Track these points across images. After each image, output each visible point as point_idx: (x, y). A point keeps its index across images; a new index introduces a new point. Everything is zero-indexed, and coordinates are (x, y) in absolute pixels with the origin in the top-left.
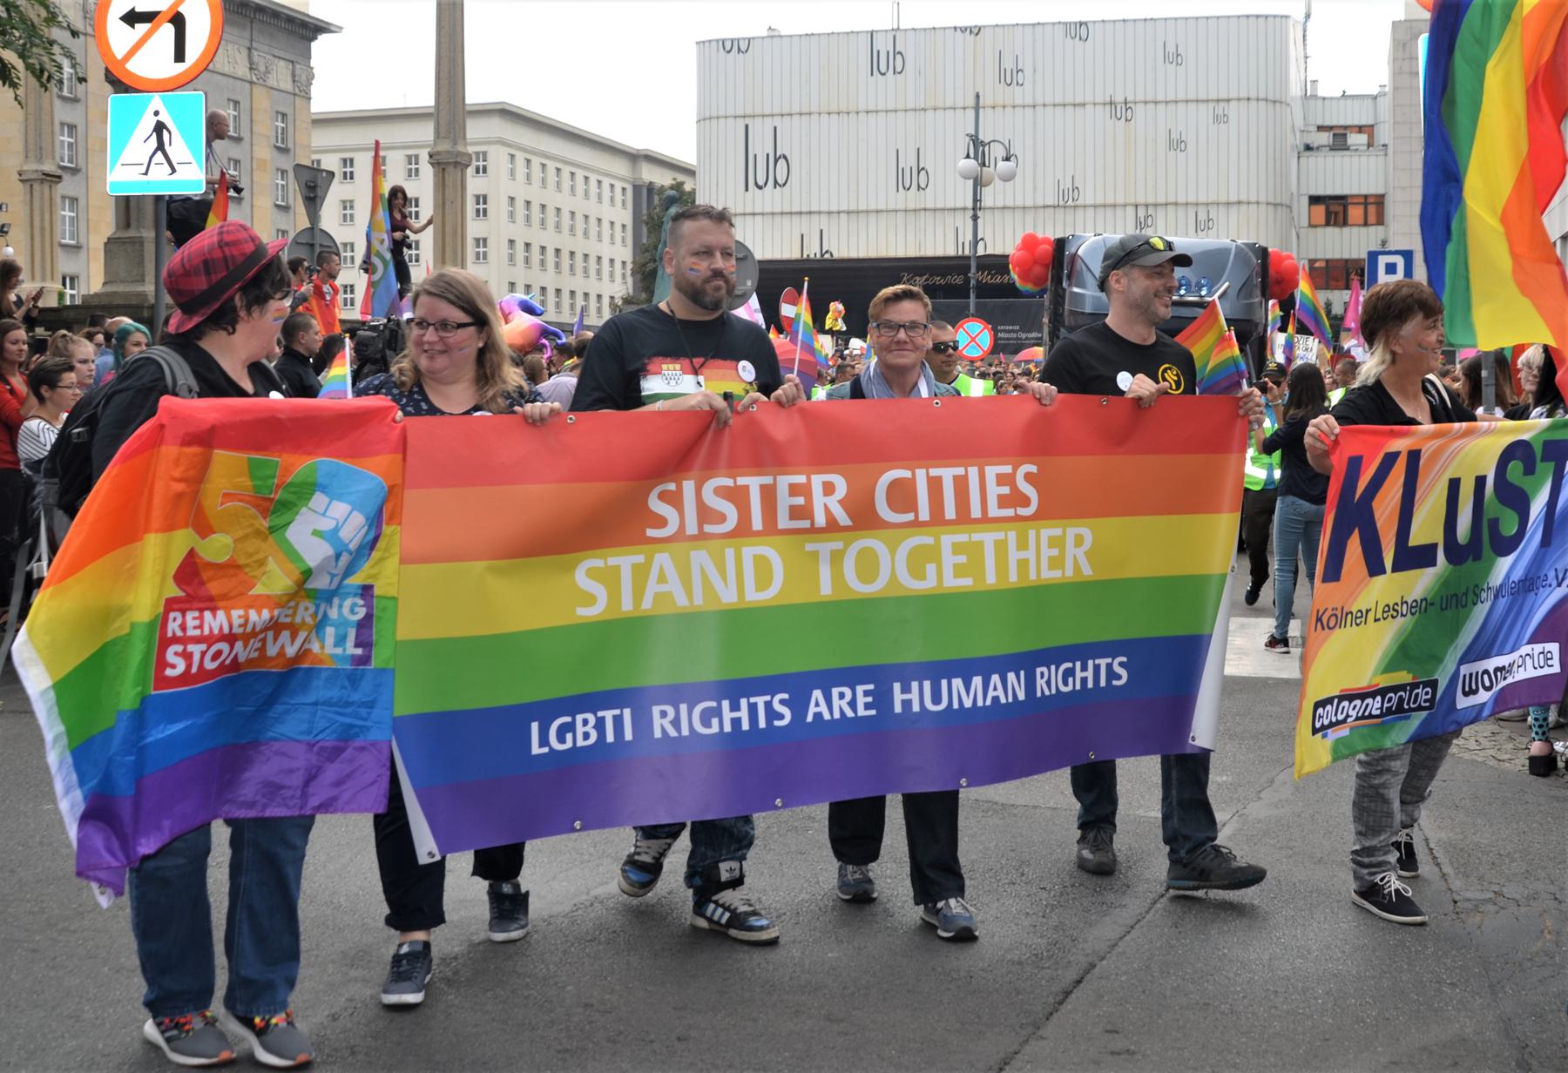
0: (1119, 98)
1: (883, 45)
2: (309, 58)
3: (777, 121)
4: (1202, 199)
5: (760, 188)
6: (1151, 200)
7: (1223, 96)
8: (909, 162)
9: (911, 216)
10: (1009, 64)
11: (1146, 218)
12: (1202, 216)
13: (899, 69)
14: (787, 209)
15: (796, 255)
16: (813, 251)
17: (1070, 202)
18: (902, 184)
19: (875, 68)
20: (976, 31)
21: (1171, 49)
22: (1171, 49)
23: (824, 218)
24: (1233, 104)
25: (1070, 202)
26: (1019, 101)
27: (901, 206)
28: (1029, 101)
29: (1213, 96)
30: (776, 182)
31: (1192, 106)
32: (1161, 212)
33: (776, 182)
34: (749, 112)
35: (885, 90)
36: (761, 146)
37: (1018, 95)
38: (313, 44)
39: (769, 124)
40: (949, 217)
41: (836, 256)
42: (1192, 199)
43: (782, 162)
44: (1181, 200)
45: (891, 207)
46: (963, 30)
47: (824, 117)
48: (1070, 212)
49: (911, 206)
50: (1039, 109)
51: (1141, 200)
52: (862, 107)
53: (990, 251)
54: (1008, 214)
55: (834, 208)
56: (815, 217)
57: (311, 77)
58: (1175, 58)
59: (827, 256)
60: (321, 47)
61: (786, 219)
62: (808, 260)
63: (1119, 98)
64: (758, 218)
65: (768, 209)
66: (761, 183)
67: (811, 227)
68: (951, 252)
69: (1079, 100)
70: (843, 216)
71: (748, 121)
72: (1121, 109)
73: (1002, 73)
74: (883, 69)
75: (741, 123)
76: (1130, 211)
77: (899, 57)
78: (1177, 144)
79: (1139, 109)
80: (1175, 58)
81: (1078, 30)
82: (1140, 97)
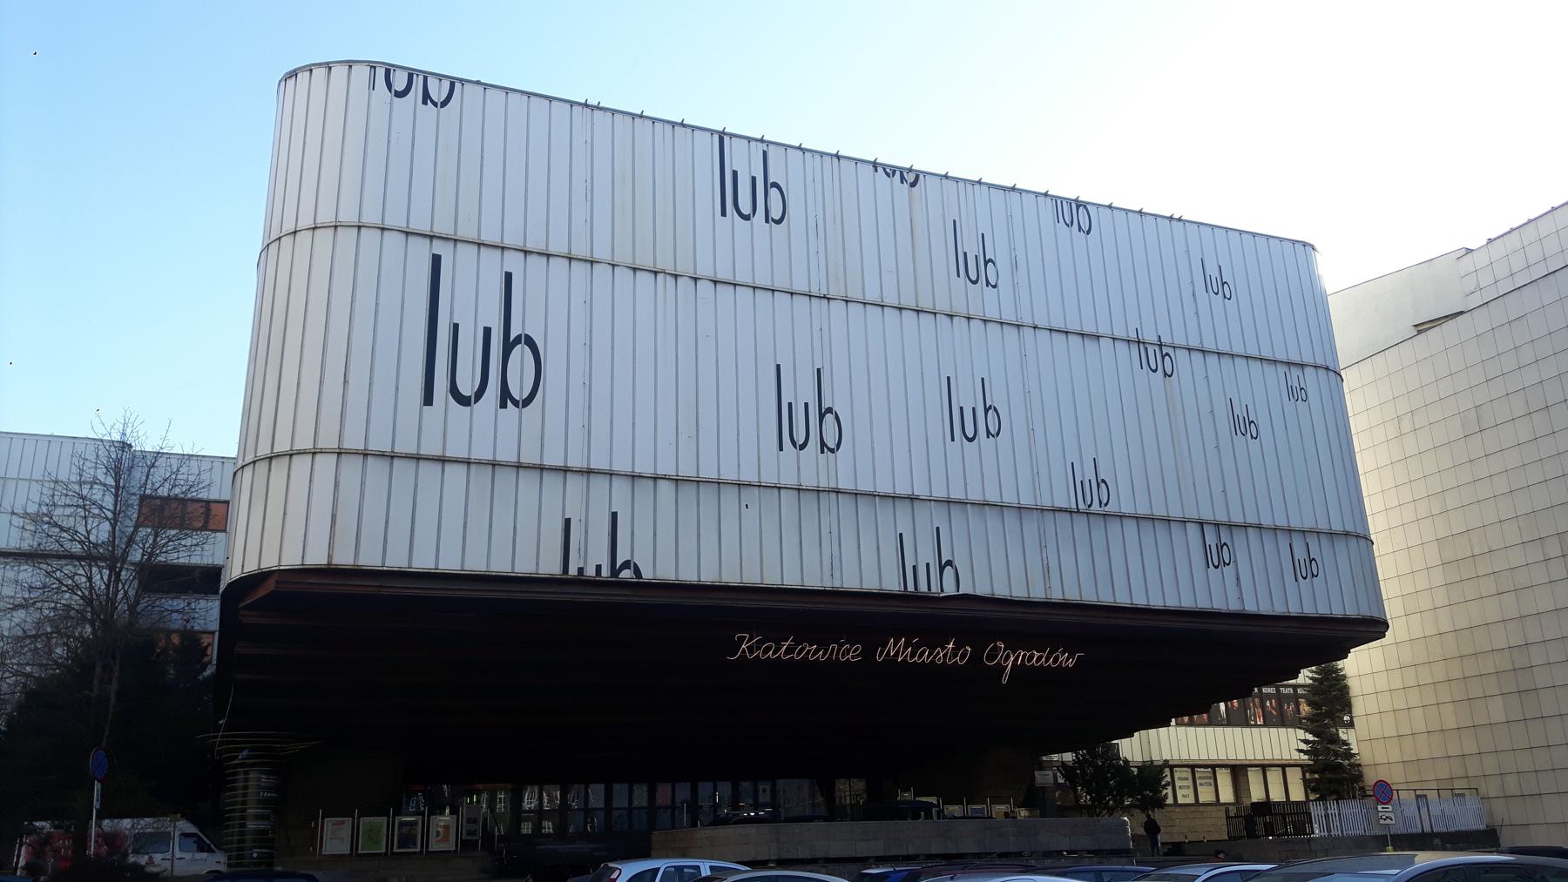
1: (744, 162)
3: (513, 262)
5: (464, 401)
8: (801, 392)
10: (971, 248)
13: (776, 213)
15: (550, 566)
16: (592, 558)
17: (1095, 507)
18: (787, 435)
19: (727, 200)
20: (911, 178)
23: (621, 487)
25: (1095, 507)
26: (992, 314)
27: (788, 479)
30: (505, 397)
32: (1239, 536)
35: (747, 247)
39: (492, 267)
40: (884, 511)
41: (647, 574)
43: (521, 354)
45: (769, 478)
46: (890, 171)
47: (623, 275)
49: (808, 481)
53: (965, 589)
55: (643, 468)
56: (599, 483)
59: (626, 574)
61: (528, 481)
62: (581, 581)
63: (1149, 336)
64: (456, 473)
65: (482, 452)
66: (466, 389)
67: (591, 508)
68: (892, 584)
71: (439, 248)
72: (1156, 354)
73: (961, 263)
74: (746, 207)
75: (421, 253)
76: (1193, 530)
77: (774, 192)
78: (1245, 426)
80: (1220, 287)
81: (1074, 212)
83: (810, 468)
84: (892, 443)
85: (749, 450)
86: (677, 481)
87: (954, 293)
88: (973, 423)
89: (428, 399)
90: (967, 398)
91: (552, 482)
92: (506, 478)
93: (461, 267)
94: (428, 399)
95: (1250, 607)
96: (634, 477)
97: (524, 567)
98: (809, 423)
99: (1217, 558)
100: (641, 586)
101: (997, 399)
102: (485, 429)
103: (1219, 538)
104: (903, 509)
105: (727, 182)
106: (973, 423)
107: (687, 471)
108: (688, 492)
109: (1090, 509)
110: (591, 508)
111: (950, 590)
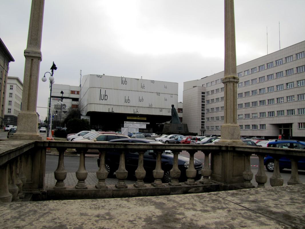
1: (124, 80)
3: (106, 89)
4: (169, 108)
5: (102, 100)
8: (127, 98)
10: (143, 85)
15: (108, 112)
16: (111, 111)
18: (125, 102)
23: (113, 106)
30: (105, 99)
33: (105, 99)
34: (101, 87)
35: (124, 87)
36: (103, 93)
39: (104, 90)
40: (133, 108)
41: (115, 112)
46: (136, 79)
48: (151, 108)
51: (161, 107)
53: (139, 113)
56: (111, 106)
66: (102, 99)
67: (110, 107)
68: (133, 113)
71: (101, 89)
72: (158, 94)
73: (142, 86)
75: (100, 89)
76: (159, 109)
78: (166, 100)
81: (153, 82)
83: (127, 104)
84: (134, 102)
85: (122, 103)
86: (117, 105)
88: (141, 100)
89: (100, 100)
92: (105, 105)
93: (102, 90)
94: (100, 100)
98: (127, 101)
99: (161, 111)
102: (104, 102)
103: (161, 109)
104: (134, 107)
105: (122, 81)
106: (141, 100)
108: (118, 106)
111: (137, 113)
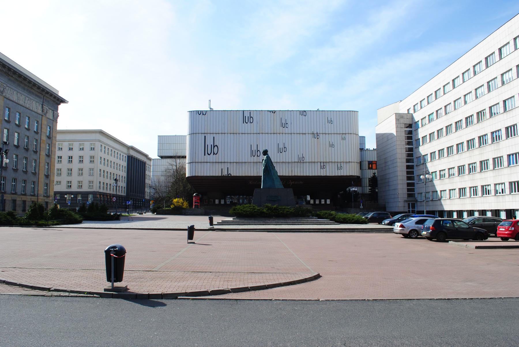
0: (315, 132)
2: (58, 110)
3: (215, 135)
4: (339, 161)
5: (209, 155)
6: (325, 161)
7: (344, 132)
9: (255, 164)
10: (284, 122)
11: (324, 166)
12: (339, 166)
14: (217, 161)
20: (274, 112)
21: (329, 119)
22: (329, 119)
23: (229, 164)
24: (347, 135)
28: (290, 132)
29: (341, 132)
30: (214, 153)
31: (336, 135)
33: (214, 153)
35: (247, 128)
36: (210, 142)
37: (286, 130)
38: (59, 106)
42: (336, 161)
43: (216, 147)
44: (333, 161)
46: (270, 111)
48: (302, 164)
50: (293, 135)
52: (241, 132)
54: (284, 164)
57: (58, 116)
58: (331, 122)
60: (61, 107)
61: (217, 164)
63: (315, 132)
66: (209, 153)
69: (304, 132)
70: (235, 164)
72: (316, 135)
74: (247, 121)
76: (319, 164)
79: (321, 135)
81: (303, 113)
82: (321, 132)
86: (236, 163)
87: (281, 130)
90: (281, 146)
91: (220, 164)
92: (214, 164)
93: (208, 136)
95: (328, 175)
96: (230, 163)
97: (217, 175)
99: (323, 167)
100: (231, 177)
101: (286, 146)
102: (212, 158)
103: (323, 165)
105: (244, 118)
107: (238, 161)
108: (238, 164)
109: (301, 161)
110: (225, 167)
